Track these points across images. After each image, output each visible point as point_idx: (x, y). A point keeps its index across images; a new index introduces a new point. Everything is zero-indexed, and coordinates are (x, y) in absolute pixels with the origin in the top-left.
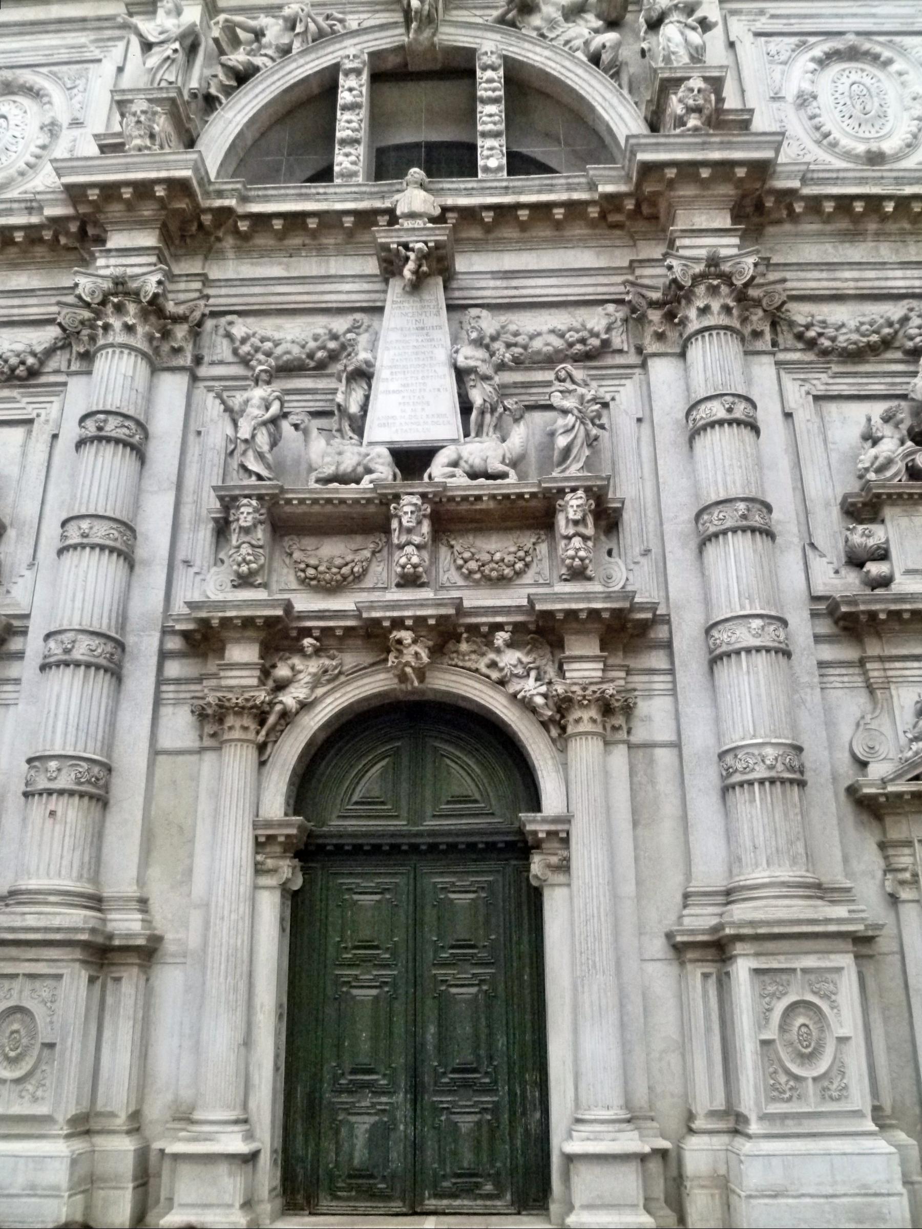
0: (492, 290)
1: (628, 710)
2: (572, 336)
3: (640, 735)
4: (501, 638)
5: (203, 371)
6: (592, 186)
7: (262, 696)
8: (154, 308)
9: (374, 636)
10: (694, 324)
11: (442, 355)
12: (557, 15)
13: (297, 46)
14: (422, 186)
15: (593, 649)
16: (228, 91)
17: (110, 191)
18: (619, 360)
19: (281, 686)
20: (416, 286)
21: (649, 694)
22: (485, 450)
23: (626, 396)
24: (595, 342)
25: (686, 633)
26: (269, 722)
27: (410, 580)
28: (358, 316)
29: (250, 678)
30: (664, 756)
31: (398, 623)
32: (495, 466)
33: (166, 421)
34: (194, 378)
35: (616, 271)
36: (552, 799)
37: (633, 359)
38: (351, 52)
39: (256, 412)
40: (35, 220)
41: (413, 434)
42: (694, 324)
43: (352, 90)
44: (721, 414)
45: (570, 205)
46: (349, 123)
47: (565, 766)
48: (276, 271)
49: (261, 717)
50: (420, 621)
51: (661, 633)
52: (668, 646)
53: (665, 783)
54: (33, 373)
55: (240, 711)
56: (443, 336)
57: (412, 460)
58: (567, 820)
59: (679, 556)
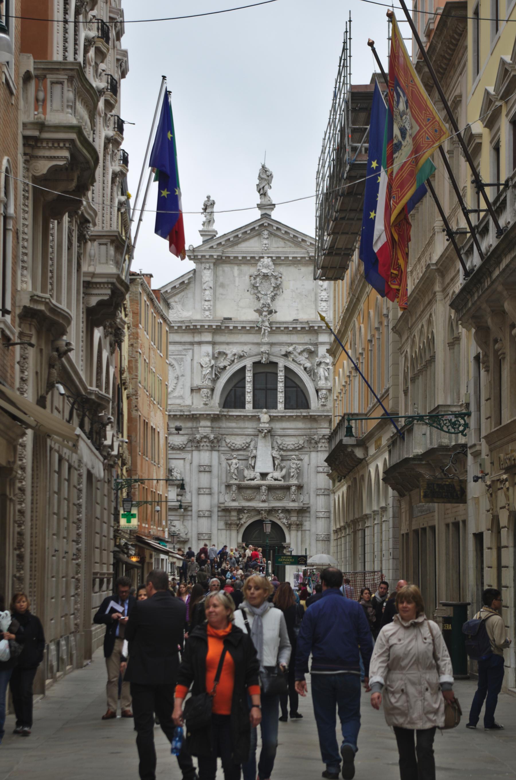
0: (280, 432)
1: (302, 525)
2: (296, 445)
3: (304, 528)
4: (280, 511)
5: (221, 449)
6: (301, 413)
7: (238, 522)
8: (212, 442)
9: (258, 511)
10: (319, 449)
11: (270, 453)
12: (297, 355)
13: (236, 361)
14: (266, 413)
15: (296, 515)
16: (220, 373)
17: (200, 414)
18: (306, 450)
19: (240, 519)
20: (265, 436)
21: (306, 521)
22: (278, 474)
23: (306, 458)
24: (300, 447)
25: (313, 510)
26: (238, 526)
27: (264, 501)
28: (252, 437)
29: (236, 518)
30: (307, 532)
31: (262, 510)
32: (280, 479)
33: (215, 463)
34: (219, 451)
35: (306, 429)
36: (288, 540)
37: (308, 449)
38: (248, 363)
39: (235, 466)
40: (182, 413)
41: (264, 471)
42: (319, 449)
43: (249, 376)
44: (322, 470)
45: (297, 416)
46: (249, 387)
47: (290, 534)
48: (233, 425)
49: (238, 525)
50: (265, 510)
51: (308, 510)
52: (310, 512)
53: (307, 537)
54: (184, 448)
55: (235, 524)
56: (270, 448)
57: (264, 475)
58: (290, 544)
59: (313, 495)
